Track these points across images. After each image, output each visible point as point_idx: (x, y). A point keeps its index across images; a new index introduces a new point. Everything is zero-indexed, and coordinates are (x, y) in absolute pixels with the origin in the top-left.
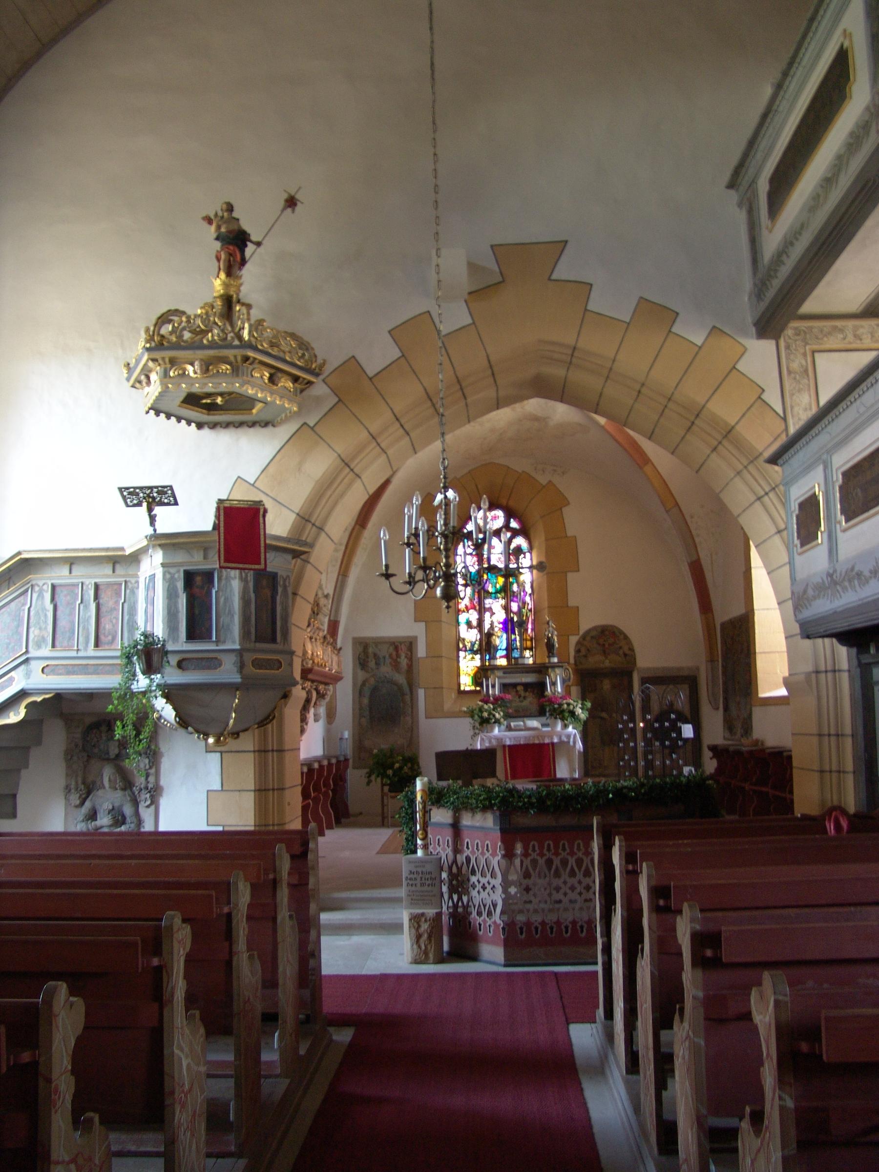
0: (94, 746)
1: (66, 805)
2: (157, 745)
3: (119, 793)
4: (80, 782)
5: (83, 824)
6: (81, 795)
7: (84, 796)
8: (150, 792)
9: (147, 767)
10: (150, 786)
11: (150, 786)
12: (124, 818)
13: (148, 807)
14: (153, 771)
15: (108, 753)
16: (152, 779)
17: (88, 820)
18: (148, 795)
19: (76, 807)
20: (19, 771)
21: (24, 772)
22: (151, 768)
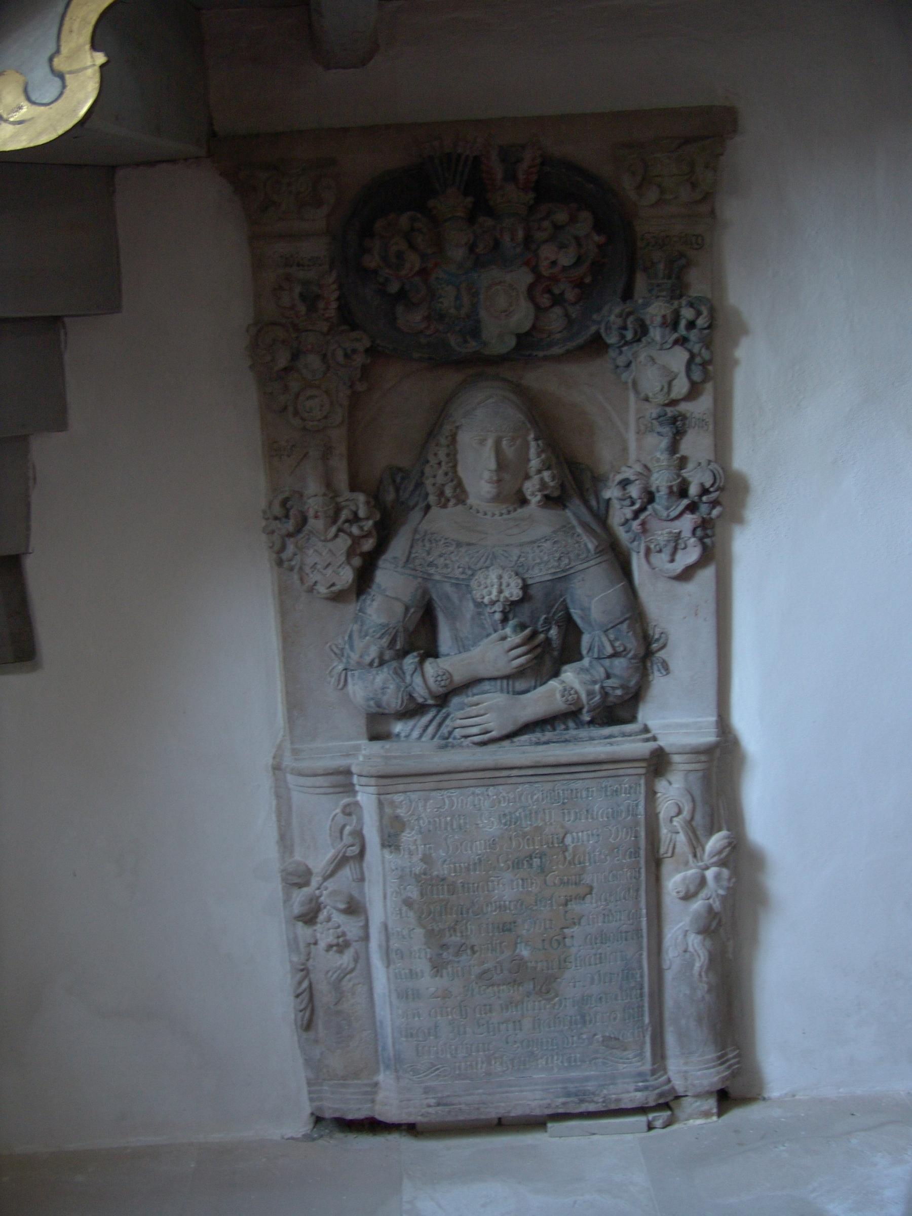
0: (402, 295)
1: (283, 593)
2: (717, 282)
3: (540, 522)
4: (342, 479)
5: (382, 677)
6: (356, 541)
7: (368, 545)
8: (692, 508)
9: (681, 386)
10: (697, 479)
11: (697, 479)
12: (571, 629)
13: (686, 575)
14: (701, 407)
15: (475, 332)
16: (697, 445)
17: (402, 654)
18: (687, 523)
19: (338, 597)
20: (23, 440)
21: (46, 451)
22: (694, 392)
